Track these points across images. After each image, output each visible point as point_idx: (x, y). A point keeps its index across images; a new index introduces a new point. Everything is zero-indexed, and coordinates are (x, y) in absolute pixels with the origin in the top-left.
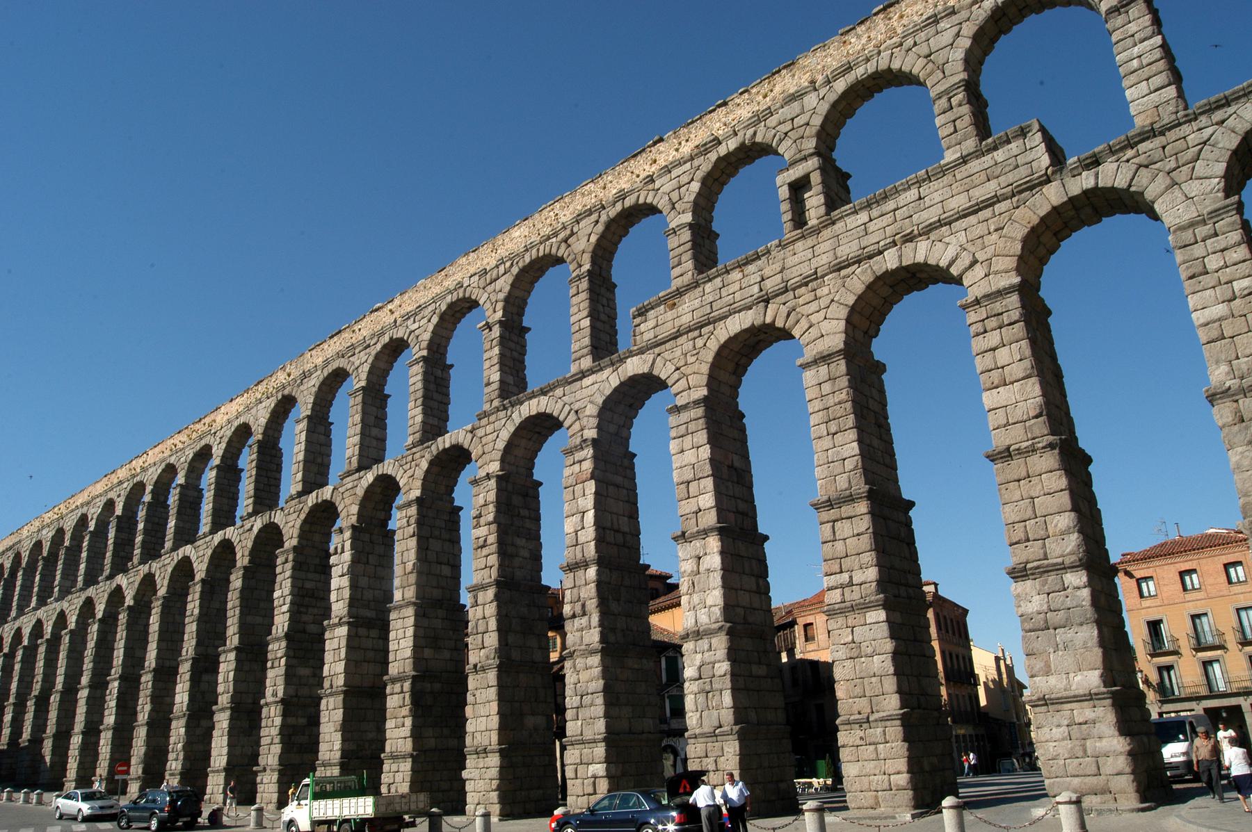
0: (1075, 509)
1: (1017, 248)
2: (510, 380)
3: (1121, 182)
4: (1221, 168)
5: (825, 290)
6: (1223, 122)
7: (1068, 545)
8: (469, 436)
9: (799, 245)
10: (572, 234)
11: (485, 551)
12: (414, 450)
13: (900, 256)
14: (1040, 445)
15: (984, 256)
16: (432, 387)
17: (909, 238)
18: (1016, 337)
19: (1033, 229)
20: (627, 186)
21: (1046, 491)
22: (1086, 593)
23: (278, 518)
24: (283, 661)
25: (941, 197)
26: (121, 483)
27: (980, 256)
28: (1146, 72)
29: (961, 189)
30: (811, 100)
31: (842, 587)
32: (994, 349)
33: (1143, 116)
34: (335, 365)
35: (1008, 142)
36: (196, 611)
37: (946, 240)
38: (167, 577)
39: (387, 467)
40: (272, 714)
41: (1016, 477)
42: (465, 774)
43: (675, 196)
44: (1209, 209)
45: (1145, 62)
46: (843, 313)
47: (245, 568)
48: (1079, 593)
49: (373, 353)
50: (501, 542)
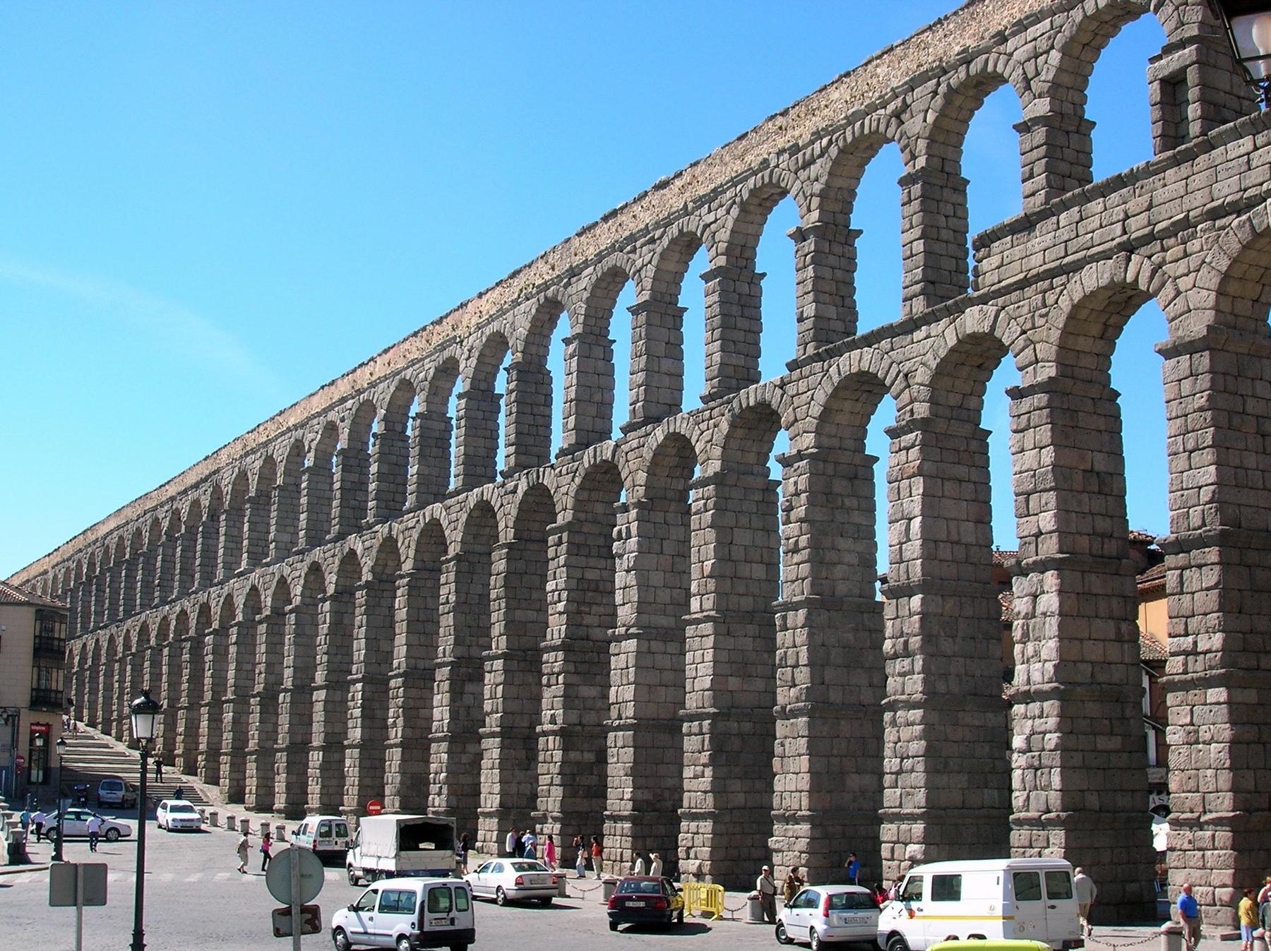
2: (832, 312)
8: (778, 392)
10: (906, 106)
11: (797, 558)
12: (712, 404)
16: (735, 310)
20: (971, 43)
23: (548, 479)
24: (561, 678)
26: (343, 400)
31: (1186, 653)
34: (609, 262)
36: (452, 598)
38: (413, 546)
39: (680, 424)
40: (551, 746)
42: (772, 842)
43: (1030, 68)
46: (1214, 282)
47: (509, 546)
49: (659, 250)
50: (814, 545)
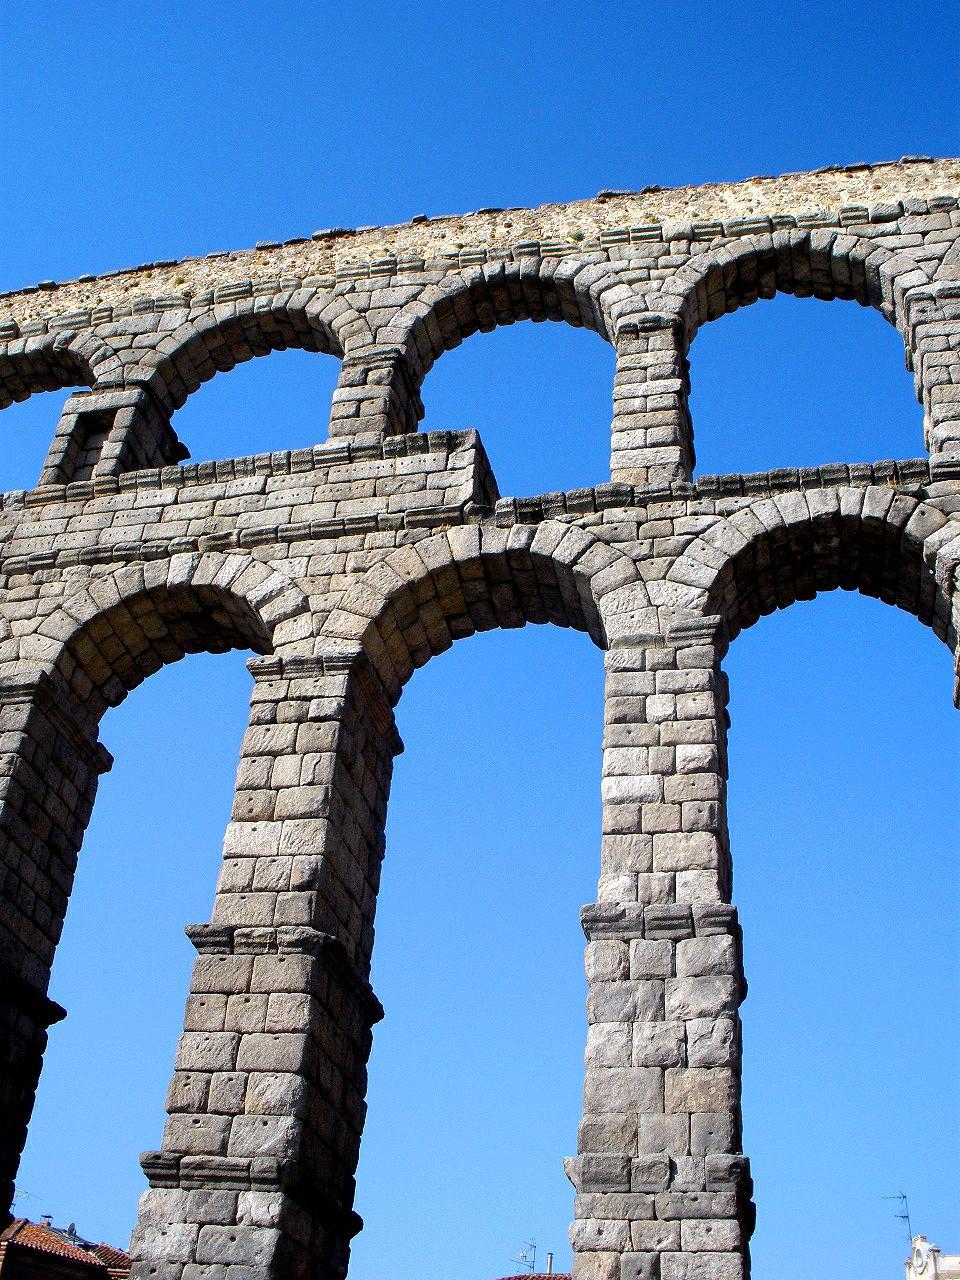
0: (308, 1070)
1: (376, 606)
3: (562, 554)
4: (708, 576)
5: (57, 587)
6: (730, 513)
7: (266, 1137)
9: (52, 509)
13: (194, 569)
14: (287, 938)
15: (325, 607)
17: (221, 544)
18: (317, 744)
19: (411, 587)
21: (268, 1025)
22: (268, 1237)
25: (297, 498)
27: (315, 603)
28: (649, 418)
29: (329, 496)
30: (174, 318)
32: (274, 754)
33: (624, 473)
35: (425, 449)
37: (274, 564)
41: (226, 986)
44: (675, 624)
45: (650, 405)
46: (67, 629)
48: (256, 1235)
